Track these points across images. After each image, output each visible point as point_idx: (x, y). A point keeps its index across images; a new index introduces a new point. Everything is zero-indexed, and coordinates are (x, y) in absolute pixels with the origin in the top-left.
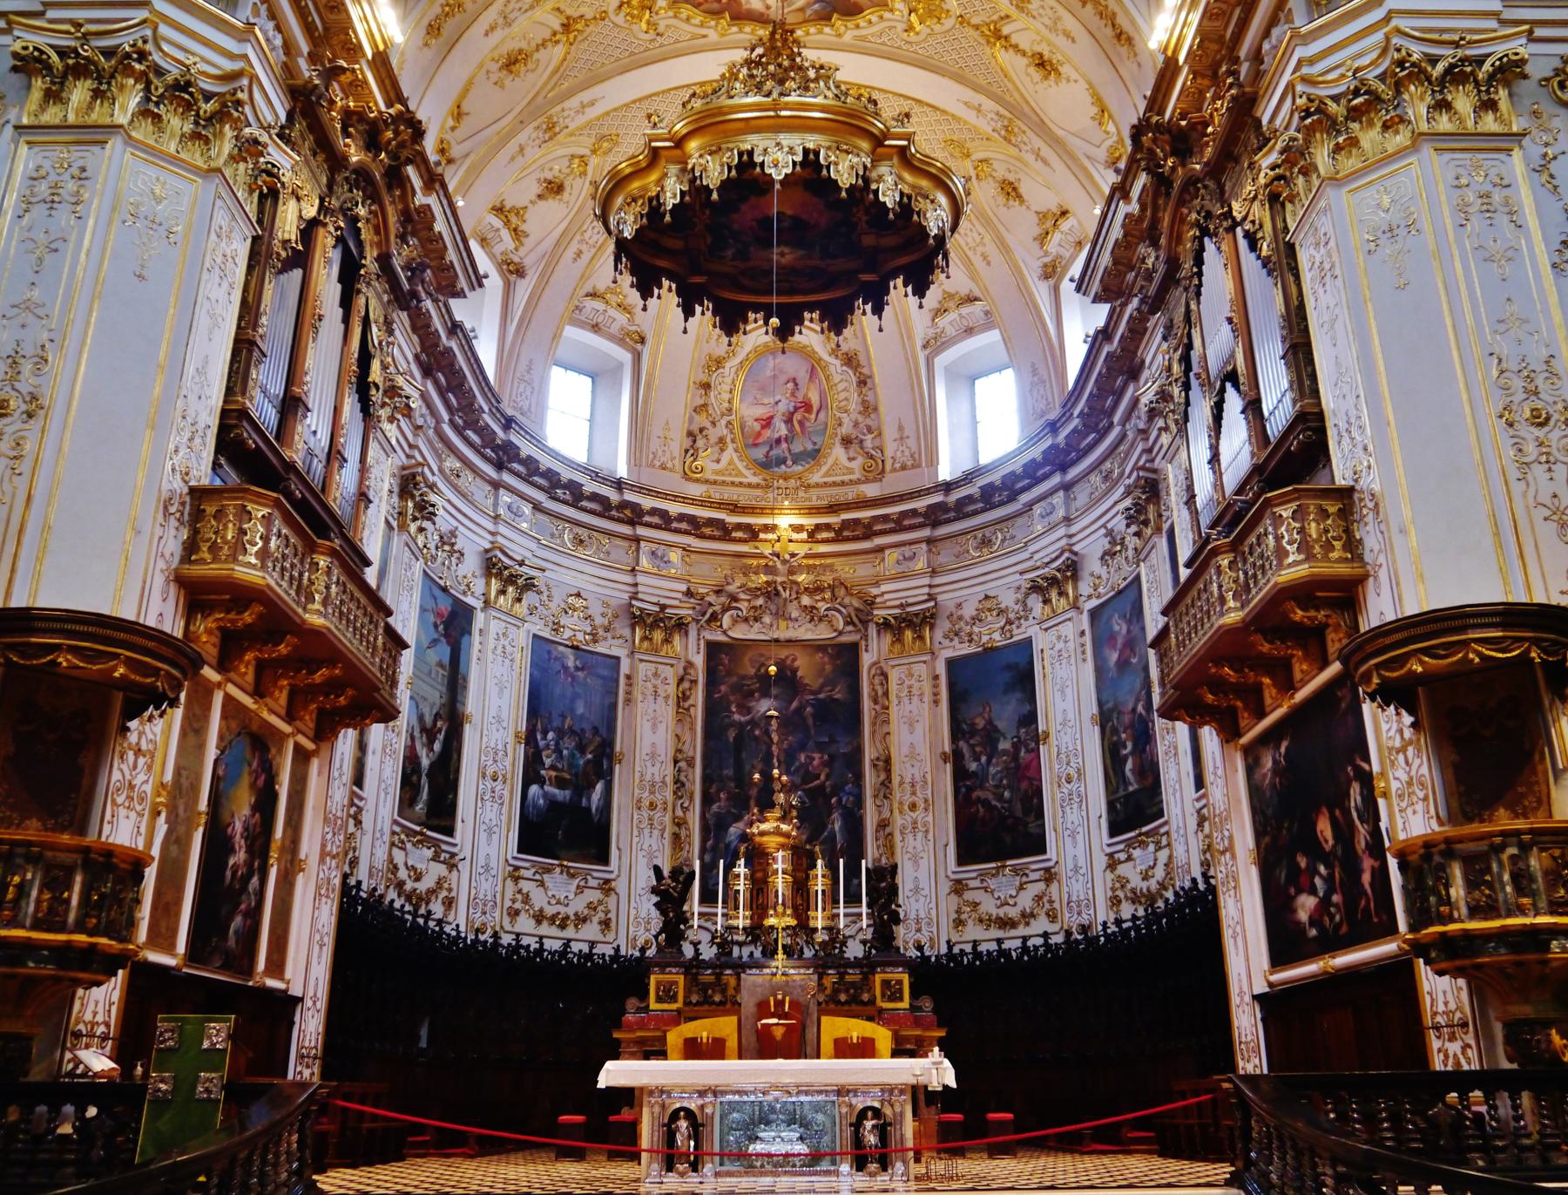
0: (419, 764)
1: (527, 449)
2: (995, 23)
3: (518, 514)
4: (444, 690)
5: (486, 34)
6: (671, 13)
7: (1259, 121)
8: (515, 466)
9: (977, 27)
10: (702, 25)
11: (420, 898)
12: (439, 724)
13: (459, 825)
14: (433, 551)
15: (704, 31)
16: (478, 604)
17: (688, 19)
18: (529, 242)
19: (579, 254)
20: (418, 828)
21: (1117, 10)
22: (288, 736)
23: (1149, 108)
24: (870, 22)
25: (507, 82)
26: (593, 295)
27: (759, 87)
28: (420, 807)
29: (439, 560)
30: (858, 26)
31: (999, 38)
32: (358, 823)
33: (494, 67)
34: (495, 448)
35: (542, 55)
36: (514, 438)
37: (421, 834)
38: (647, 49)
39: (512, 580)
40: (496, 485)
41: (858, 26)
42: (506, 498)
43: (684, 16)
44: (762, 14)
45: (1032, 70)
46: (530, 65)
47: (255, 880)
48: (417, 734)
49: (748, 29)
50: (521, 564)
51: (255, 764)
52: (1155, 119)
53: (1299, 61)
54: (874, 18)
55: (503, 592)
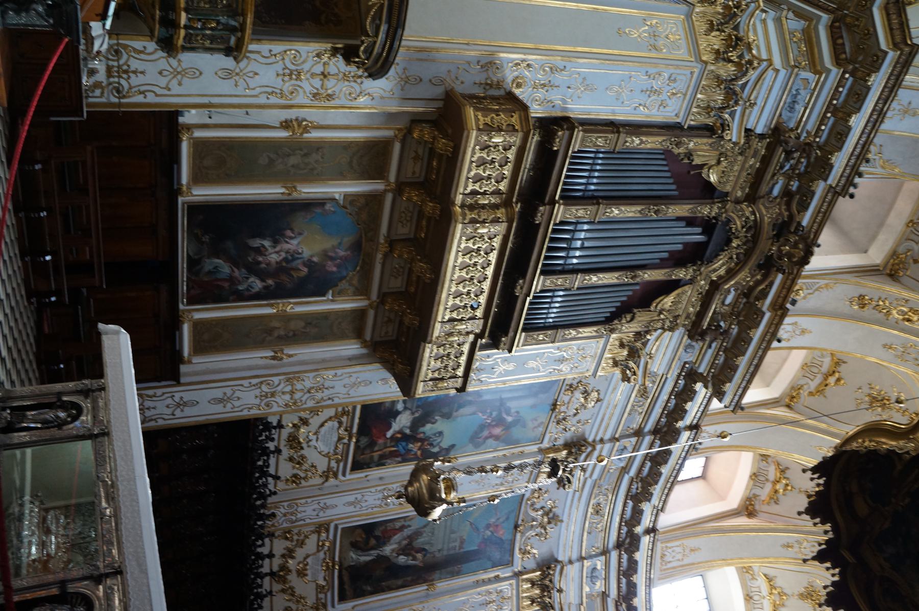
0: (384, 544)
1: (641, 556)
3: (593, 577)
4: (445, 553)
5: (885, 346)
8: (625, 557)
11: (284, 580)
12: (419, 556)
13: (349, 605)
14: (538, 506)
16: (518, 567)
18: (774, 508)
19: (788, 546)
20: (337, 559)
22: (369, 299)
26: (769, 579)
28: (354, 557)
29: (533, 514)
32: (326, 475)
33: (866, 390)
34: (630, 534)
36: (646, 540)
37: (333, 566)
39: (545, 589)
40: (605, 552)
42: (599, 563)
47: (257, 285)
48: (407, 532)
50: (560, 591)
51: (342, 253)
55: (533, 583)
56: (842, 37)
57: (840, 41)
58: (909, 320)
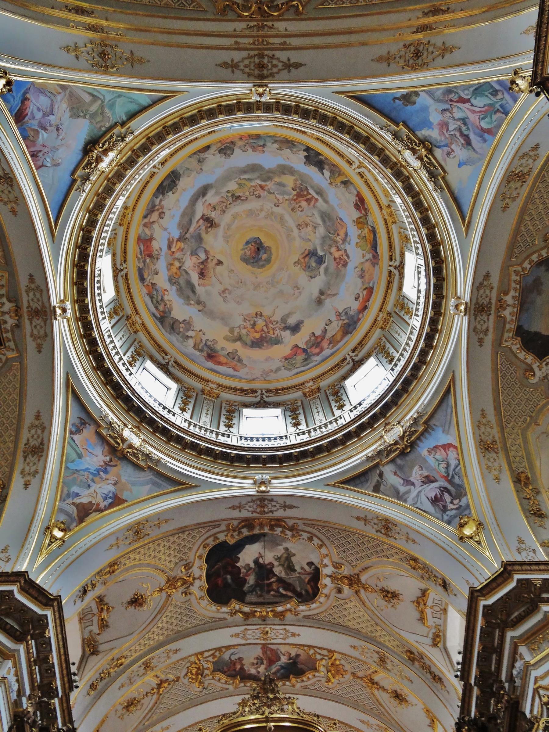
2: (370, 675)
5: (119, 689)
6: (211, 677)
7: (524, 714)
9: (362, 678)
10: (226, 683)
15: (226, 686)
17: (219, 679)
21: (430, 664)
23: (462, 712)
24: (309, 678)
25: (125, 716)
27: (257, 710)
30: (303, 681)
31: (373, 683)
35: (146, 701)
38: (199, 696)
41: (303, 681)
43: (217, 679)
44: (256, 676)
45: (392, 700)
46: (139, 707)
49: (248, 684)
52: (467, 718)
53: (536, 679)
54: (310, 676)
56: (7, 623)
57: (8, 626)
58: (121, 665)
